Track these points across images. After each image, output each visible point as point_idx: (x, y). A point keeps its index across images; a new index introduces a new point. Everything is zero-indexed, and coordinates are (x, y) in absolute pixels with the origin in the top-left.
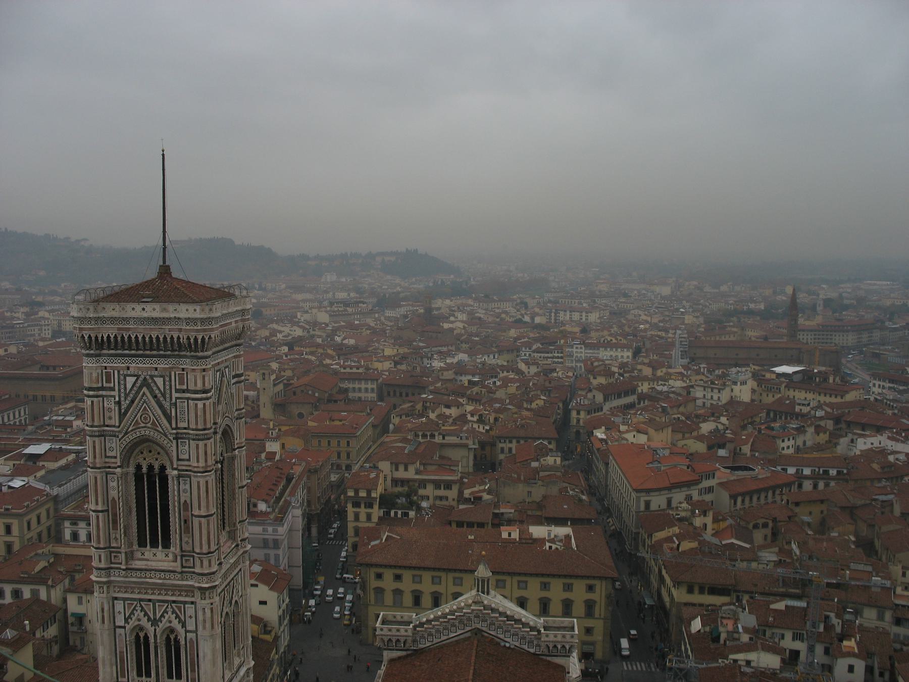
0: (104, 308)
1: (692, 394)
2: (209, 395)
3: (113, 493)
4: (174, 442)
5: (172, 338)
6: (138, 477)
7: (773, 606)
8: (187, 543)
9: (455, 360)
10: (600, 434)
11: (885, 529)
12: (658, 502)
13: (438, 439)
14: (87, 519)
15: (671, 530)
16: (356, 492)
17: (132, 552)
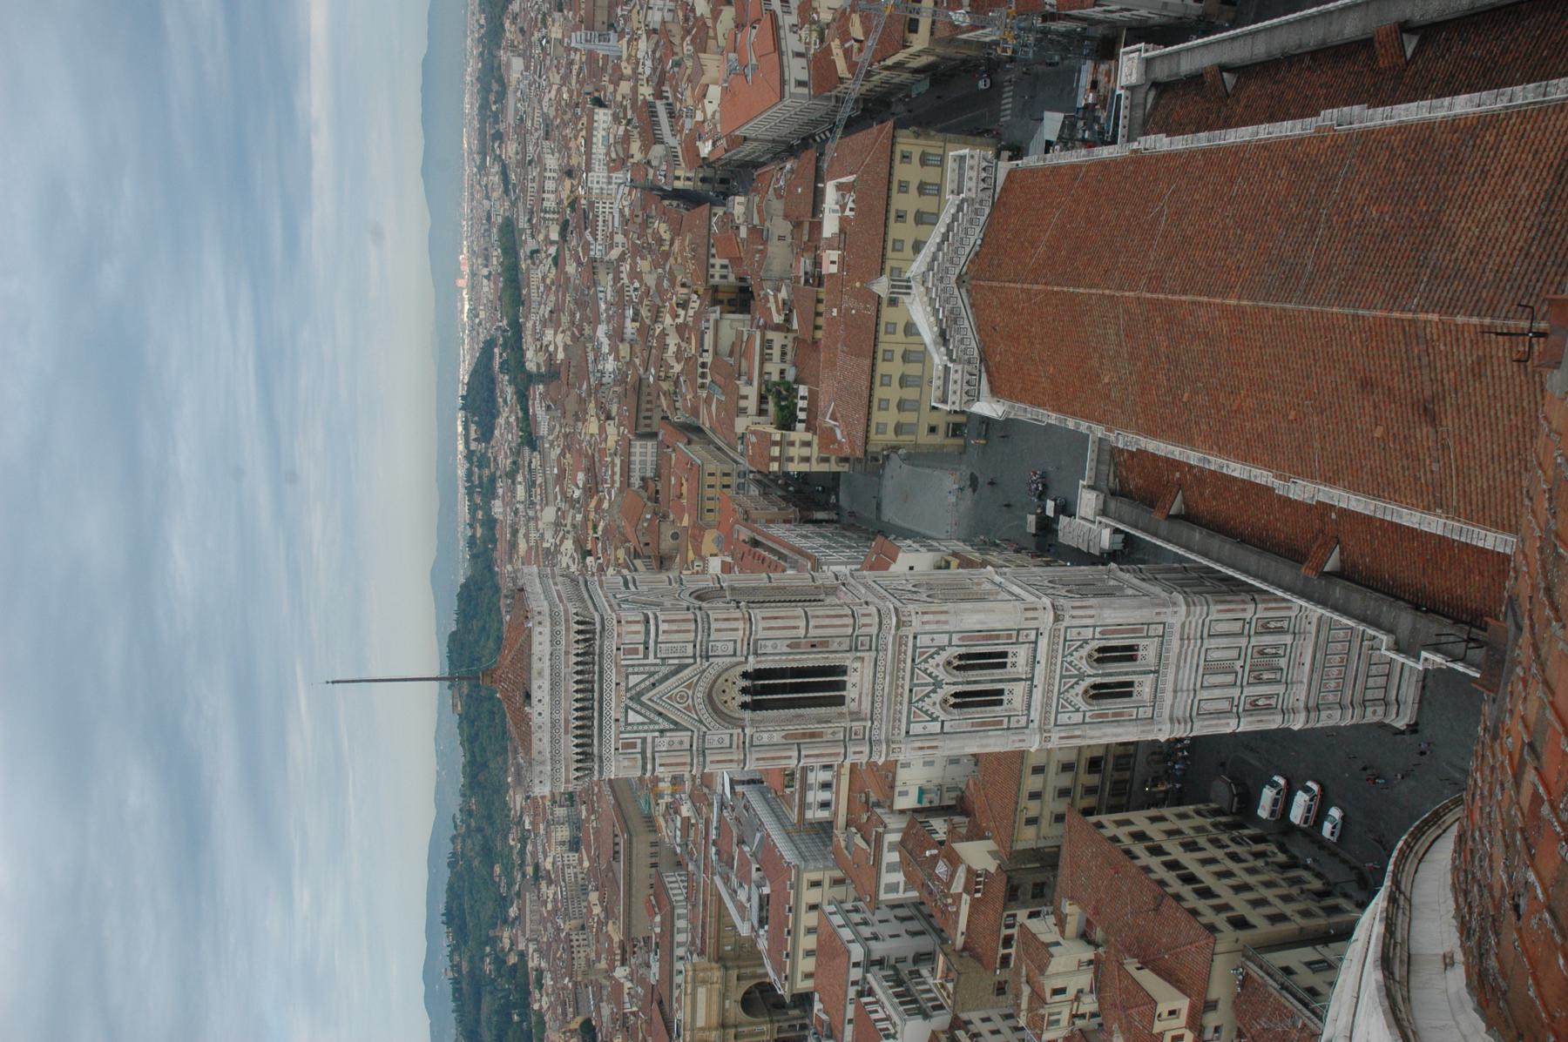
1: (657, 26)
2: (651, 616)
3: (777, 737)
4: (711, 660)
5: (577, 664)
6: (756, 706)
8: (840, 644)
9: (606, 342)
10: (705, 149)
12: (797, 70)
13: (708, 358)
14: (805, 770)
15: (835, 51)
16: (774, 459)
17: (851, 713)
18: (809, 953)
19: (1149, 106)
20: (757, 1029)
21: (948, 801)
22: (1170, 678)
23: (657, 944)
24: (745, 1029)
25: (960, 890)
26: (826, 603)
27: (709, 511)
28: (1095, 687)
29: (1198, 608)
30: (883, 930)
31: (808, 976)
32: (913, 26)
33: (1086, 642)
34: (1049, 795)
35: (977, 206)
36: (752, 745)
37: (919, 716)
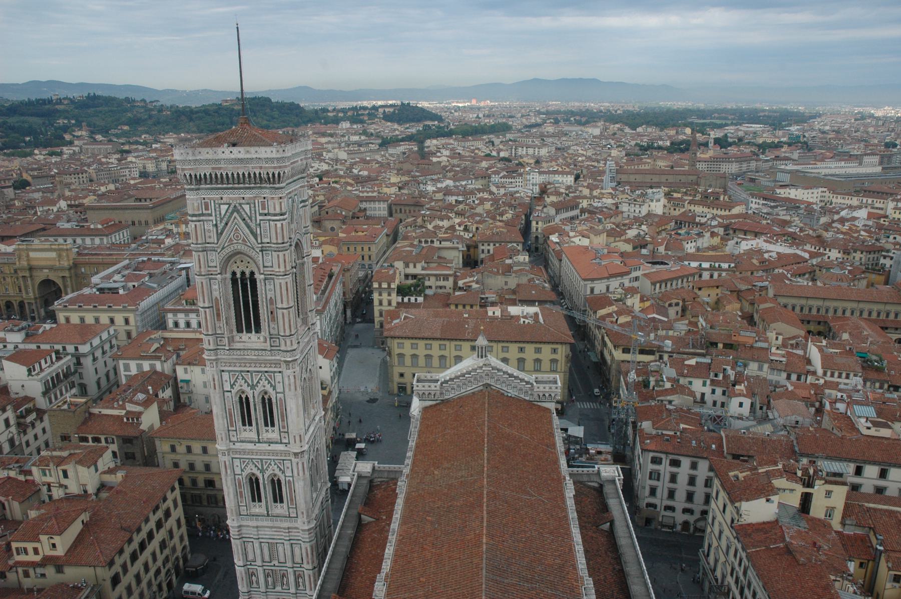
0: (200, 153)
1: (620, 209)
2: (285, 217)
3: (216, 294)
4: (260, 253)
5: (255, 173)
6: (234, 281)
7: (686, 362)
8: (274, 328)
9: (444, 185)
11: (762, 306)
12: (600, 287)
13: (436, 244)
14: (197, 311)
15: (611, 308)
16: (380, 285)
17: (233, 337)
18: (82, 319)
19: (590, 484)
21: (184, 398)
22: (265, 523)
23: (83, 226)
25: (128, 409)
26: (297, 319)
27: (348, 248)
28: (257, 479)
29: (307, 536)
30: (100, 364)
31: (67, 320)
32: (626, 351)
33: (283, 472)
34: (190, 458)
35: (529, 392)
36: (210, 279)
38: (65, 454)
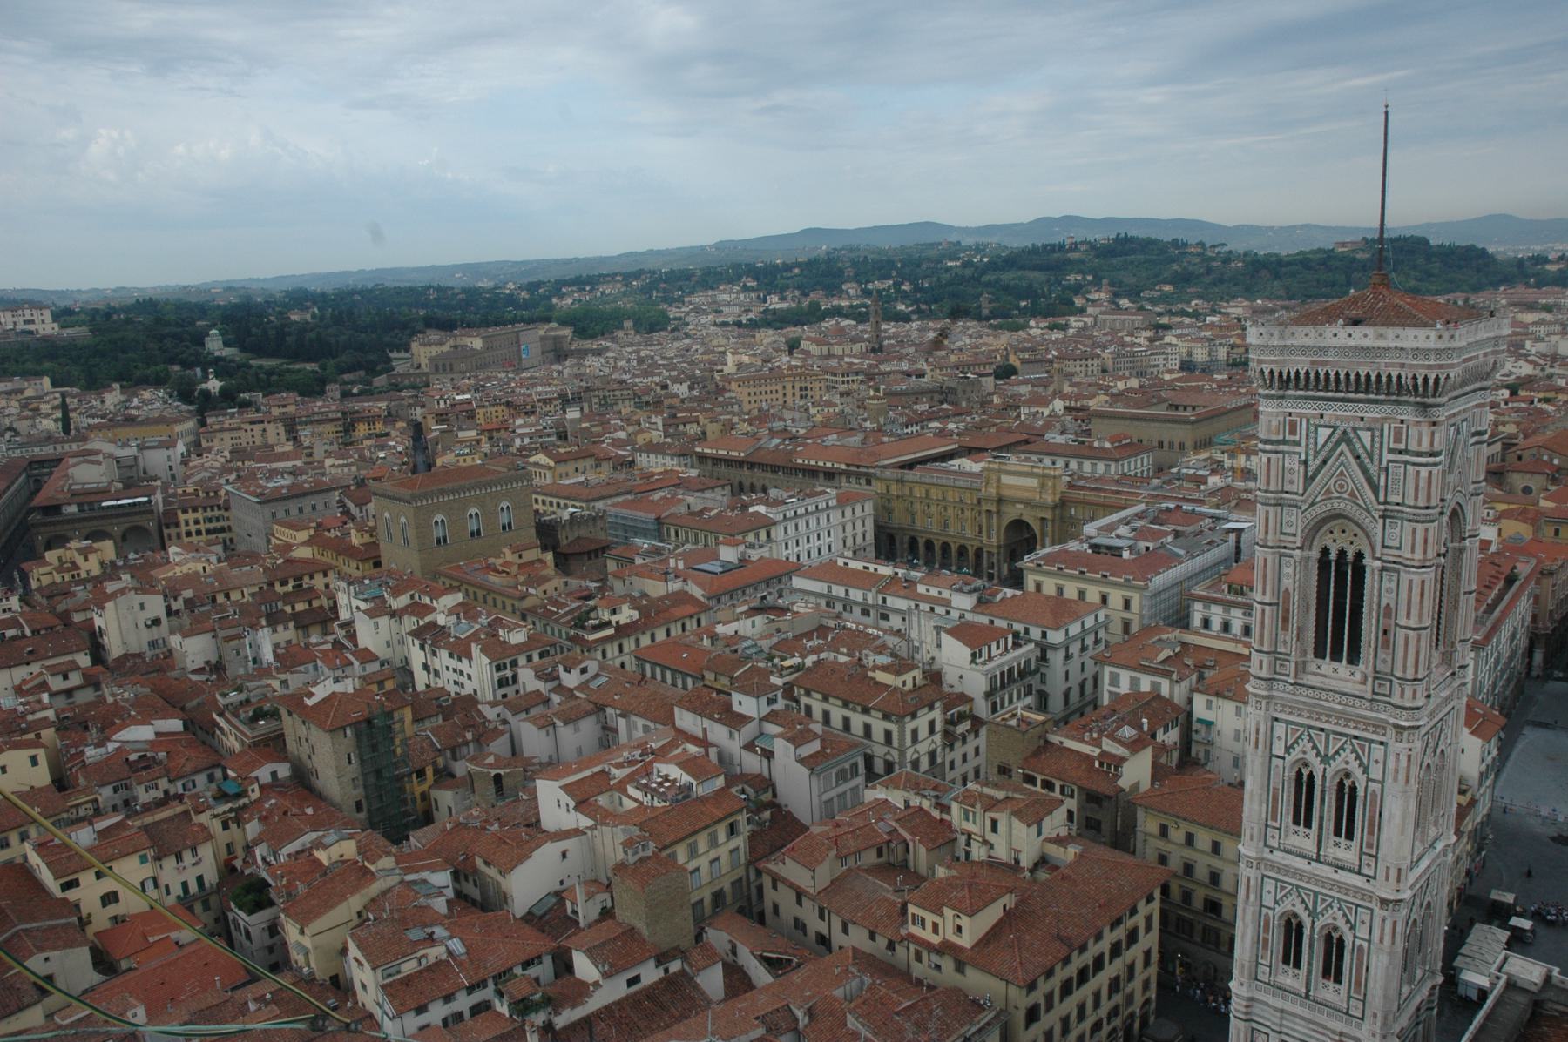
2: (1438, 459)
3: (1287, 583)
4: (1381, 521)
5: (1389, 376)
6: (1324, 563)
8: (1384, 661)
14: (1247, 609)
17: (1304, 663)
18: (1060, 590)
20: (994, 533)
22: (1298, 1010)
23: (1083, 442)
24: (995, 521)
25: (1104, 747)
26: (1433, 651)
28: (1300, 926)
30: (1074, 665)
31: (1038, 586)
33: (1353, 928)
34: (1188, 853)
36: (1281, 555)
37: (1293, 734)
38: (1000, 795)
